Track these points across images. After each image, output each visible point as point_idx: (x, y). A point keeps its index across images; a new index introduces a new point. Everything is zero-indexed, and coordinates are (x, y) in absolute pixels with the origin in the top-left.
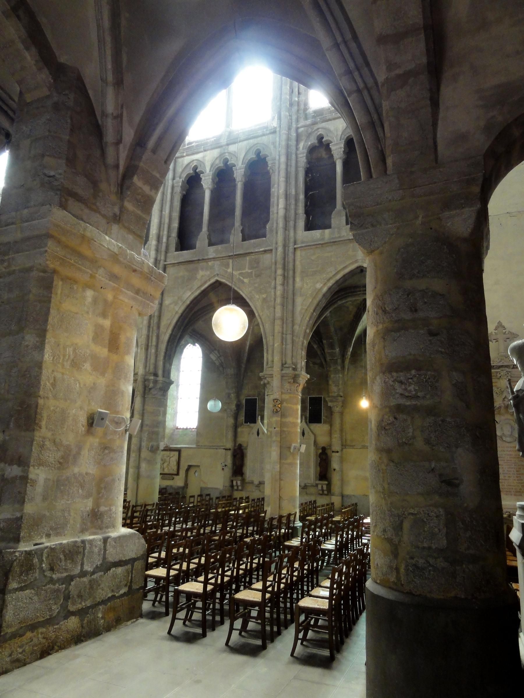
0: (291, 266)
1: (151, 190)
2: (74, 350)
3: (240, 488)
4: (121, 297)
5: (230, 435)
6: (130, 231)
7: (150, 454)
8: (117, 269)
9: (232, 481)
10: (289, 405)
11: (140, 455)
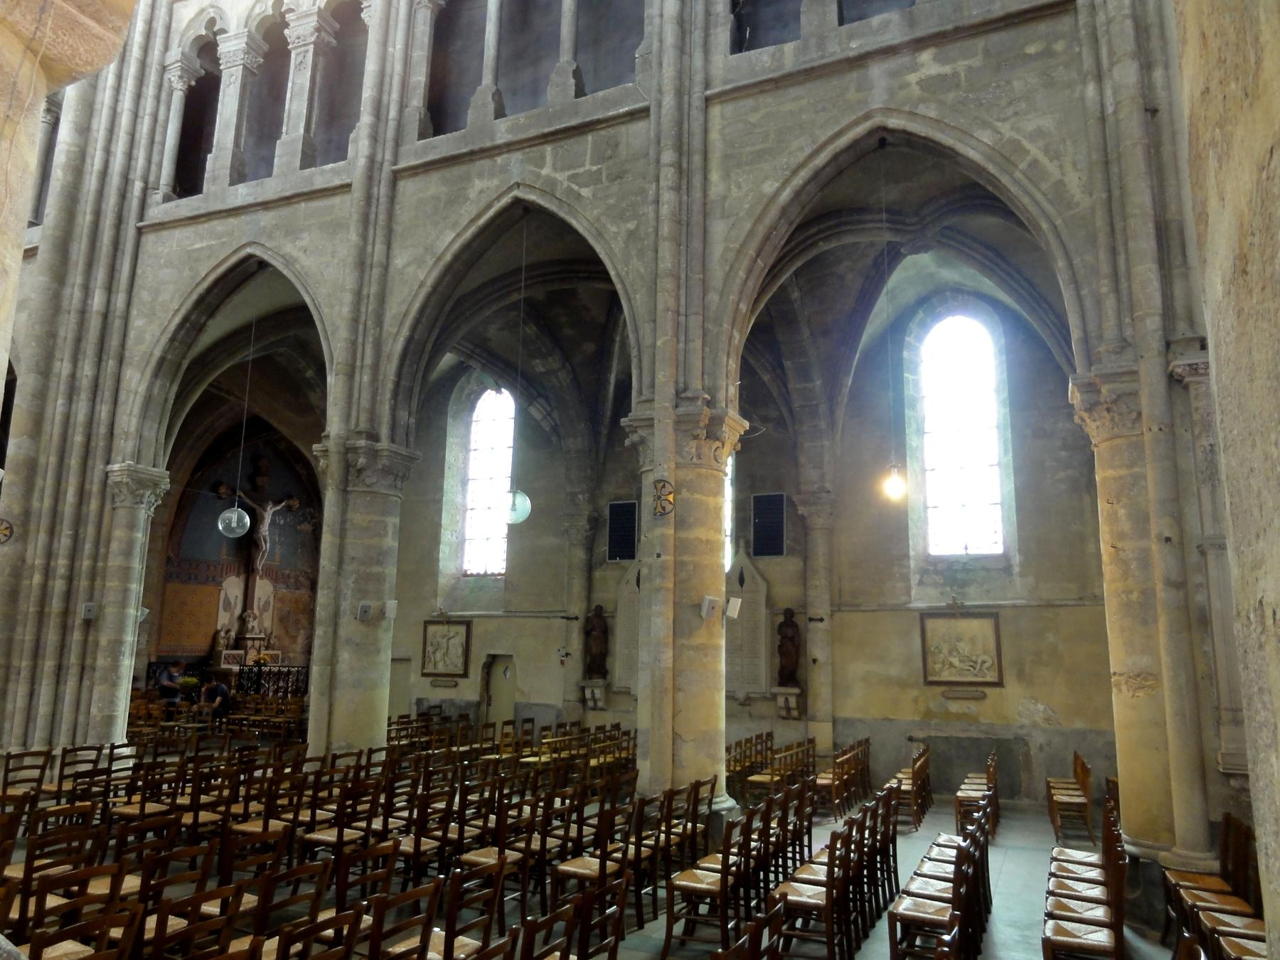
0: (697, 143)
3: (600, 704)
5: (578, 585)
9: (583, 689)
10: (697, 496)
11: (335, 632)
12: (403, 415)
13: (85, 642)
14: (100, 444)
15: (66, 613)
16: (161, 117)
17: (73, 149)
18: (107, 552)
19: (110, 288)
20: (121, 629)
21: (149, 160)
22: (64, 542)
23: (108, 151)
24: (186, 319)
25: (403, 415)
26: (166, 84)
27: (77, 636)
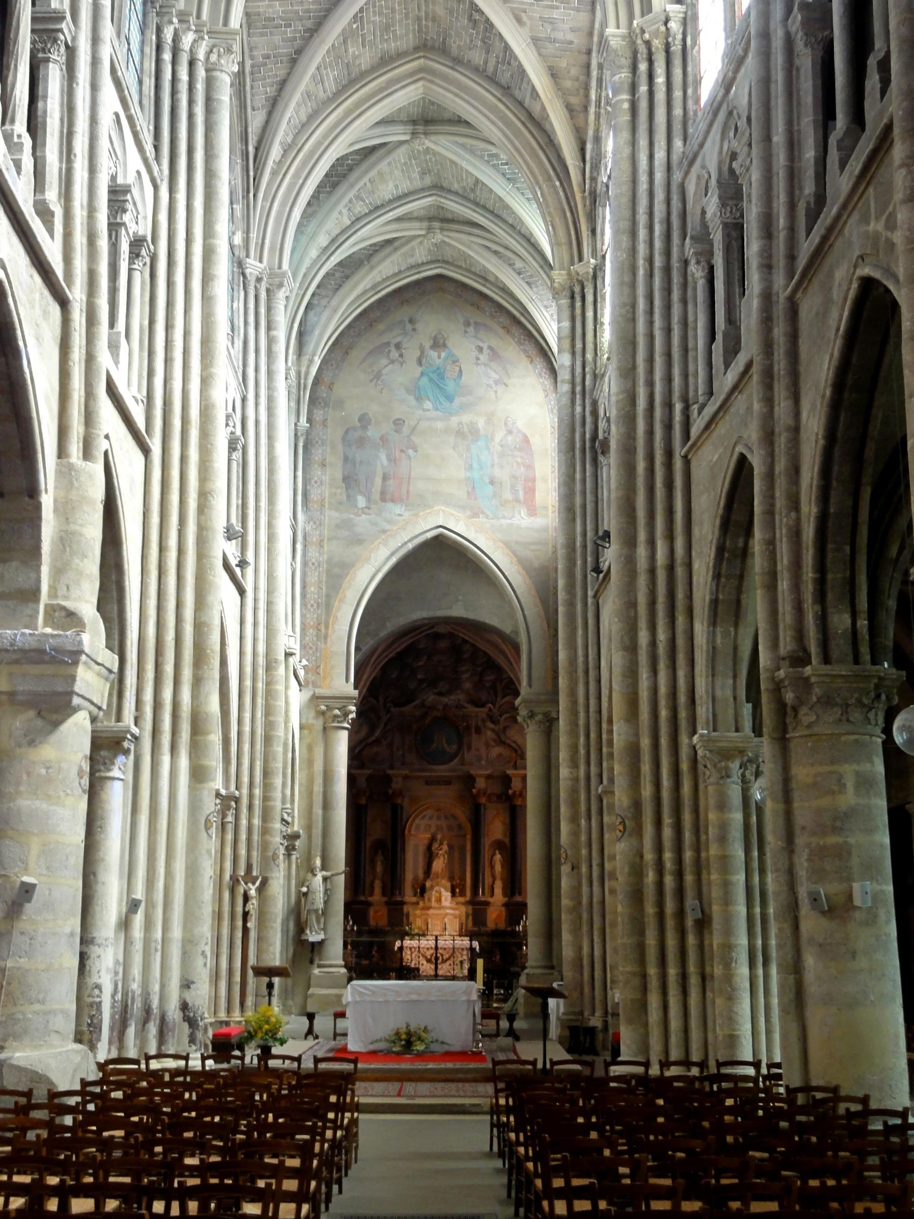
7: (824, 922)
11: (796, 927)
12: (841, 621)
13: (701, 946)
14: (683, 714)
15: (680, 913)
16: (691, 318)
17: (621, 397)
18: (707, 839)
19: (670, 537)
20: (728, 931)
21: (685, 375)
22: (667, 833)
23: (650, 384)
24: (721, 550)
25: (841, 621)
26: (690, 278)
27: (691, 940)
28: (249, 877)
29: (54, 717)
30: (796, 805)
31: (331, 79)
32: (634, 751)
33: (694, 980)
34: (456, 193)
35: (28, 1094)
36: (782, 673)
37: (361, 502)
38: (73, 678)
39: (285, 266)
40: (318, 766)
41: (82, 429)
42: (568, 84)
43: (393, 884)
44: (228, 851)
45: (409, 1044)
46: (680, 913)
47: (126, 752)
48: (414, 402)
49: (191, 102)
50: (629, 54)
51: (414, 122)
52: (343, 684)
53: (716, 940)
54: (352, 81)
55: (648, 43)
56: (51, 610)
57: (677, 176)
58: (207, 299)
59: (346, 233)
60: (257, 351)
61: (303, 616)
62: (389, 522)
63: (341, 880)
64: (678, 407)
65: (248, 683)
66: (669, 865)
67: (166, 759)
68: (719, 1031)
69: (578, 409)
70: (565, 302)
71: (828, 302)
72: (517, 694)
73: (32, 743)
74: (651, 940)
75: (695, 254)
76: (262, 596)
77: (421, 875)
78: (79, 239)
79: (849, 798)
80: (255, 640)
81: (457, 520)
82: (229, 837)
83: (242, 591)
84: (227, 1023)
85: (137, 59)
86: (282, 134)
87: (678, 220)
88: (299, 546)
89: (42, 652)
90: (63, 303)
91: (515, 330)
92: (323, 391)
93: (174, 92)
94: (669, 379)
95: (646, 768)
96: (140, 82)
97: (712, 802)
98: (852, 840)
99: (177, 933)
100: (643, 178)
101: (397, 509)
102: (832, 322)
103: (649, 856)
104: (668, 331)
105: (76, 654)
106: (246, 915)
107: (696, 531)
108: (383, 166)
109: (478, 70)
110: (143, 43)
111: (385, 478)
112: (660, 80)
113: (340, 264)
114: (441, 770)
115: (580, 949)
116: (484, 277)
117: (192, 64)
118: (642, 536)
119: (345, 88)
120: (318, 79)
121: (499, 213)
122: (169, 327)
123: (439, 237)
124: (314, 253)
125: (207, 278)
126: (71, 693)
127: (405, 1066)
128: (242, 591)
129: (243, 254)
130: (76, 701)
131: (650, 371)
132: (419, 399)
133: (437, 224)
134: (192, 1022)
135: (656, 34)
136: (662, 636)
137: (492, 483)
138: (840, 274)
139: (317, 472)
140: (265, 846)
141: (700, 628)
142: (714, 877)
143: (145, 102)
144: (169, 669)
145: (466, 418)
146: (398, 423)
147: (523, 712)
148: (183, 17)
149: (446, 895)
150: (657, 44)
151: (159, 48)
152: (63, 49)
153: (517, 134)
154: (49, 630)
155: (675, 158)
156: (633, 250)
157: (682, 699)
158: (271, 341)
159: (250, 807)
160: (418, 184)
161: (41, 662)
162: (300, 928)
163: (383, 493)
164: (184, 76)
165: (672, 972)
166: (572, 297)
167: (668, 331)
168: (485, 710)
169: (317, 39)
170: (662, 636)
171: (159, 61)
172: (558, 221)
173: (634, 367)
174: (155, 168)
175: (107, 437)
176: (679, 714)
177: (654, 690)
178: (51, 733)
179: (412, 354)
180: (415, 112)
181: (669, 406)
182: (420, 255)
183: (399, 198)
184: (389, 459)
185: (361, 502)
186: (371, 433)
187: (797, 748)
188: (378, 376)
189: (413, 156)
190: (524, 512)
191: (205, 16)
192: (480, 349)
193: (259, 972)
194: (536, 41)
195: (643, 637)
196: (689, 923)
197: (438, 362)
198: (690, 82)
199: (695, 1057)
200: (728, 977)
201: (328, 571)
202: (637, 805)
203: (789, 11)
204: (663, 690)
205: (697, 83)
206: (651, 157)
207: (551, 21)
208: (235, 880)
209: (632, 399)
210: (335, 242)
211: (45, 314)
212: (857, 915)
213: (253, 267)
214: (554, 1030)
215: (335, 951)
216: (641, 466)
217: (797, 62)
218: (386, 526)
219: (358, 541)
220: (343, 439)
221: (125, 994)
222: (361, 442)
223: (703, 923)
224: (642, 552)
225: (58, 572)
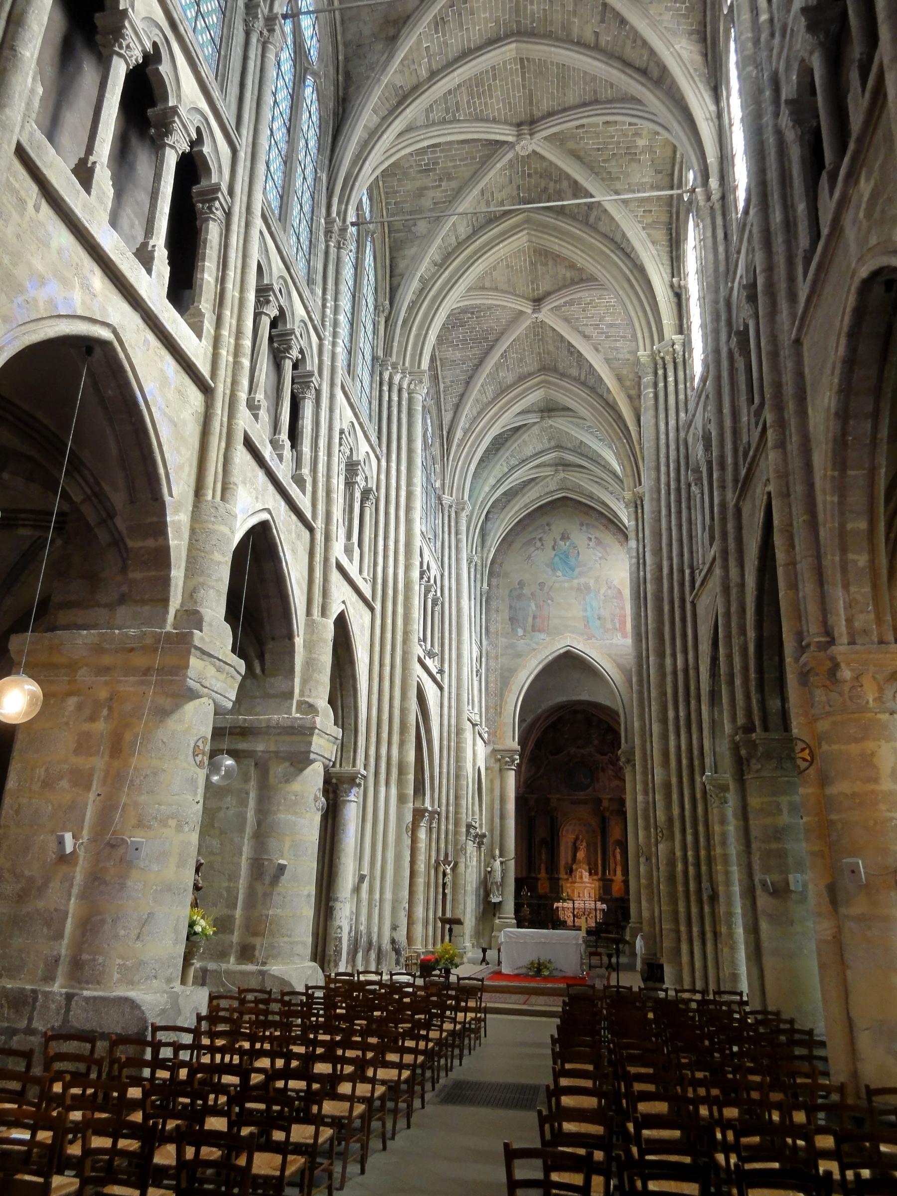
1: (156, 540)
2: (47, 770)
4: (121, 688)
6: (143, 602)
8: (106, 660)
13: (713, 914)
15: (699, 891)
19: (685, 651)
20: (730, 903)
21: (691, 552)
22: (689, 838)
23: (670, 558)
27: (707, 909)
28: (446, 862)
29: (300, 766)
30: (751, 822)
31: (490, 391)
32: (667, 786)
33: (709, 936)
34: (570, 449)
35: (269, 993)
36: (737, 738)
37: (520, 632)
38: (310, 743)
39: (466, 498)
40: (497, 793)
41: (321, 600)
42: (628, 383)
43: (552, 866)
44: (434, 845)
45: (539, 971)
46: (699, 891)
47: (359, 785)
48: (550, 572)
49: (399, 412)
50: (652, 365)
51: (542, 411)
52: (512, 743)
53: (722, 909)
54: (503, 391)
55: (663, 359)
56: (300, 703)
57: (682, 434)
58: (409, 521)
59: (506, 476)
60: (450, 547)
61: (486, 701)
62: (537, 644)
63: (512, 863)
64: (687, 572)
65: (445, 743)
66: (691, 859)
67: (383, 789)
68: (726, 972)
69: (642, 573)
70: (632, 510)
71: (754, 506)
72: (619, 747)
73: (287, 781)
74: (682, 909)
75: (695, 480)
76: (454, 690)
77: (570, 861)
78: (321, 493)
79: (785, 818)
80: (449, 717)
81: (579, 642)
82: (434, 836)
83: (441, 688)
84: (433, 953)
85: (368, 391)
86: (463, 423)
87: (684, 460)
88: (483, 659)
89: (293, 728)
90: (311, 530)
91: (611, 526)
92: (497, 568)
93: (389, 407)
94: (681, 555)
95: (675, 797)
96: (370, 403)
97: (716, 819)
98: (788, 846)
99: (388, 895)
100: (663, 437)
101: (542, 636)
102: (756, 520)
103: (678, 853)
104: (680, 526)
105: (312, 729)
106: (444, 885)
107: (700, 647)
108: (525, 437)
109: (577, 380)
110: (372, 382)
111: (534, 618)
112: (671, 379)
113: (505, 494)
114: (581, 795)
115: (653, 912)
116: (591, 497)
117: (400, 390)
118: (668, 651)
119: (498, 395)
120: (483, 391)
121: (596, 459)
122: (386, 538)
123: (562, 475)
124: (487, 489)
125: (409, 509)
126: (309, 752)
127: (533, 985)
128: (441, 688)
129: (441, 493)
130: (312, 756)
131: (670, 551)
132: (554, 570)
133: (560, 468)
134: (397, 952)
135: (667, 353)
136: (682, 714)
137: (599, 618)
138: (759, 490)
139: (494, 615)
140: (456, 842)
141: (705, 708)
142: (719, 867)
143: (373, 414)
144: (385, 735)
145: (582, 580)
146: (542, 585)
147: (623, 759)
148: (394, 366)
149: (586, 874)
150: (668, 358)
151: (381, 384)
152: (313, 391)
153: (600, 414)
154: (298, 715)
155: (681, 423)
156: (658, 479)
157: (696, 752)
158: (458, 541)
159: (447, 818)
160: (547, 446)
161: (293, 734)
162: (487, 893)
163: (533, 626)
164: (395, 398)
165: (695, 930)
166: (636, 507)
167: (680, 526)
168: (607, 757)
169: (480, 370)
170: (682, 714)
171: (381, 391)
172: (626, 462)
173: (661, 549)
174: (378, 450)
175: (344, 602)
176: (694, 763)
177: (679, 747)
178: (297, 775)
179: (549, 543)
180: (542, 405)
181: (682, 571)
182: (552, 486)
183: (536, 454)
184: (536, 605)
185: (520, 632)
186: (526, 591)
187: (752, 786)
188: (529, 557)
189: (543, 430)
190: (619, 635)
191: (407, 364)
192: (590, 539)
193: (444, 921)
194: (607, 360)
195: (671, 714)
196: (705, 897)
197: (565, 548)
198: (688, 378)
199: (699, 986)
200: (731, 935)
201: (501, 674)
202: (670, 820)
203: (729, 337)
204: (683, 747)
205: (693, 379)
206: (667, 424)
207: (616, 349)
208: (437, 863)
209: (660, 568)
210: (499, 482)
211: (299, 536)
212: (793, 896)
213: (447, 499)
214: (639, 966)
215: (509, 908)
216: (666, 608)
217: (736, 365)
218: (536, 647)
219: (519, 656)
220: (509, 596)
221: (356, 933)
222: (520, 597)
223: (714, 898)
224: (668, 661)
225: (305, 681)
